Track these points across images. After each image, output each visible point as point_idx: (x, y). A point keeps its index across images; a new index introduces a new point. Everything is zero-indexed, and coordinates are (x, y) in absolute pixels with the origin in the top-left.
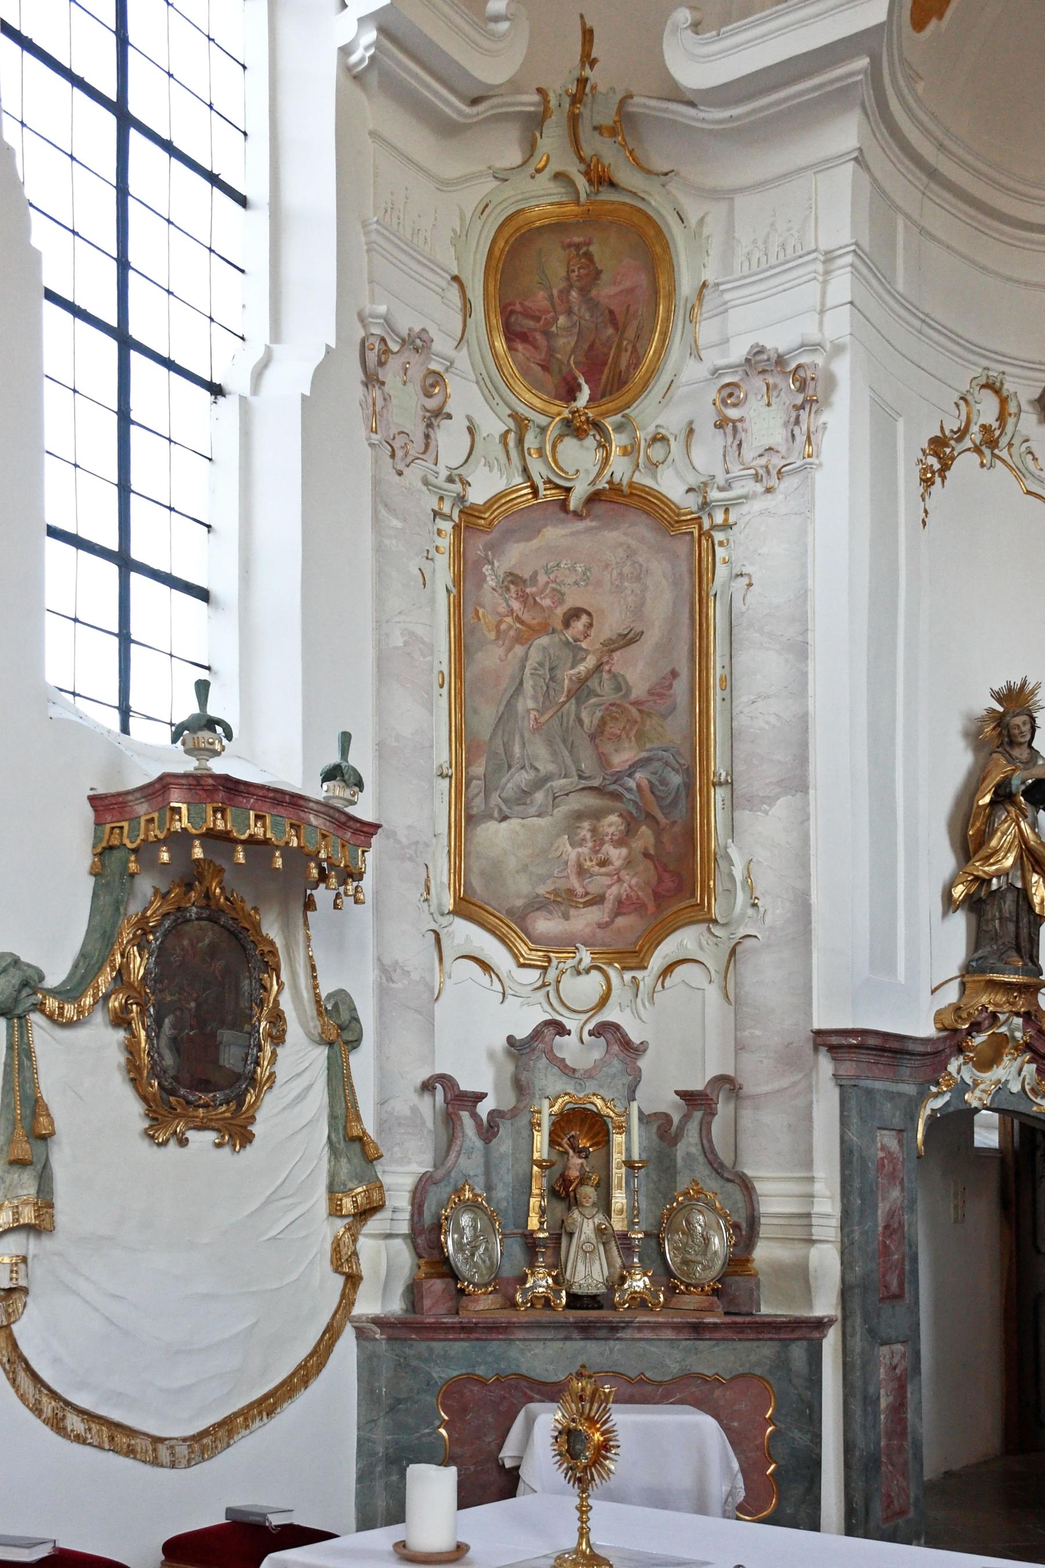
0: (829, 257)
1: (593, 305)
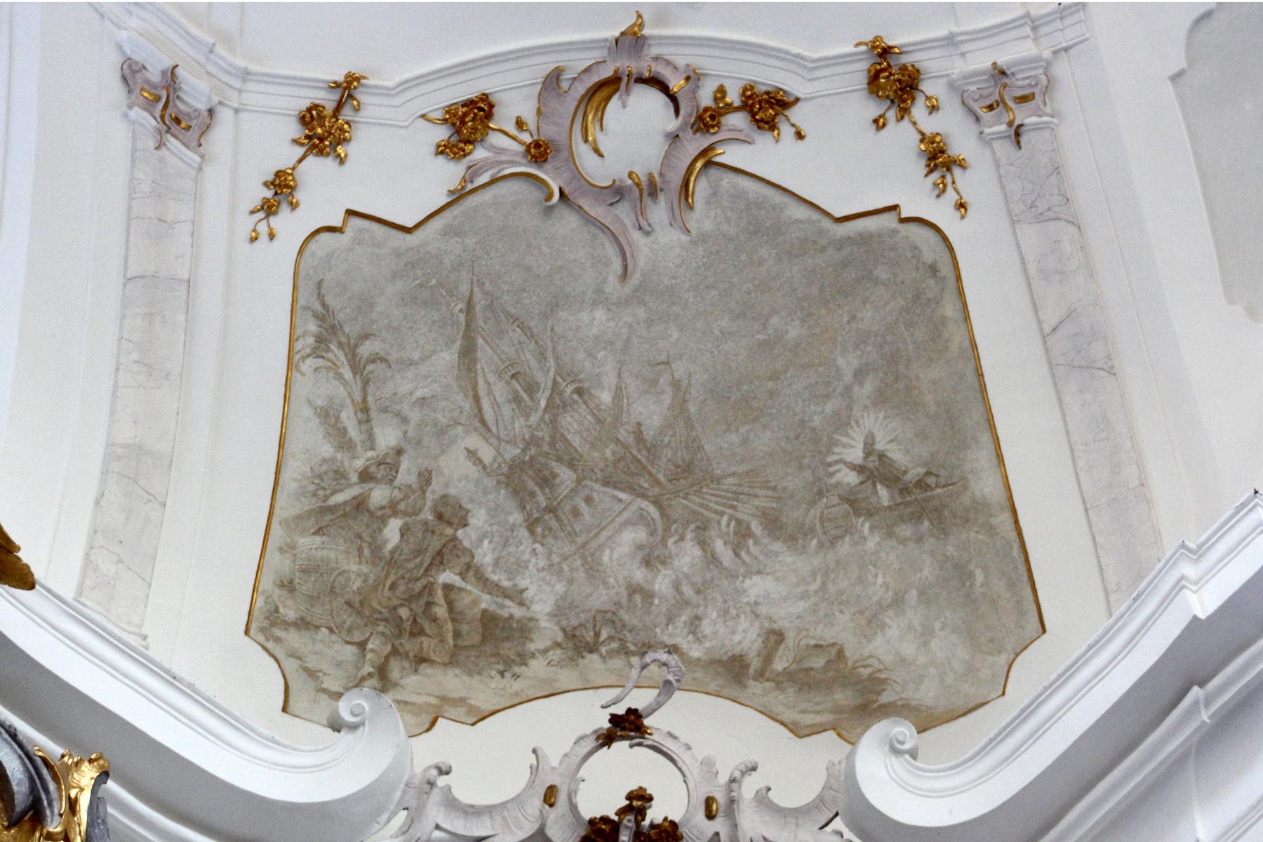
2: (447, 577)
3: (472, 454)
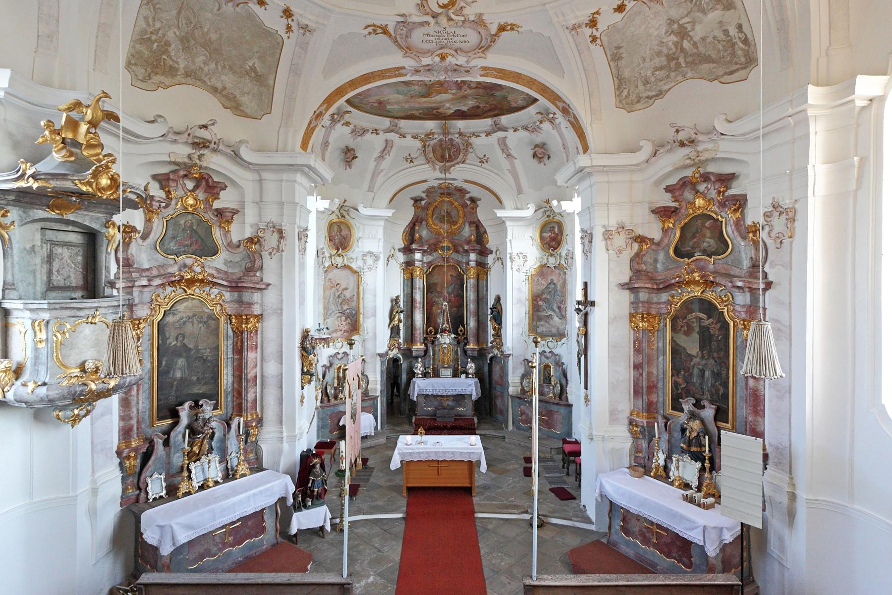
0: (380, 239)
1: (341, 235)
2: (164, 57)
3: (175, 33)
